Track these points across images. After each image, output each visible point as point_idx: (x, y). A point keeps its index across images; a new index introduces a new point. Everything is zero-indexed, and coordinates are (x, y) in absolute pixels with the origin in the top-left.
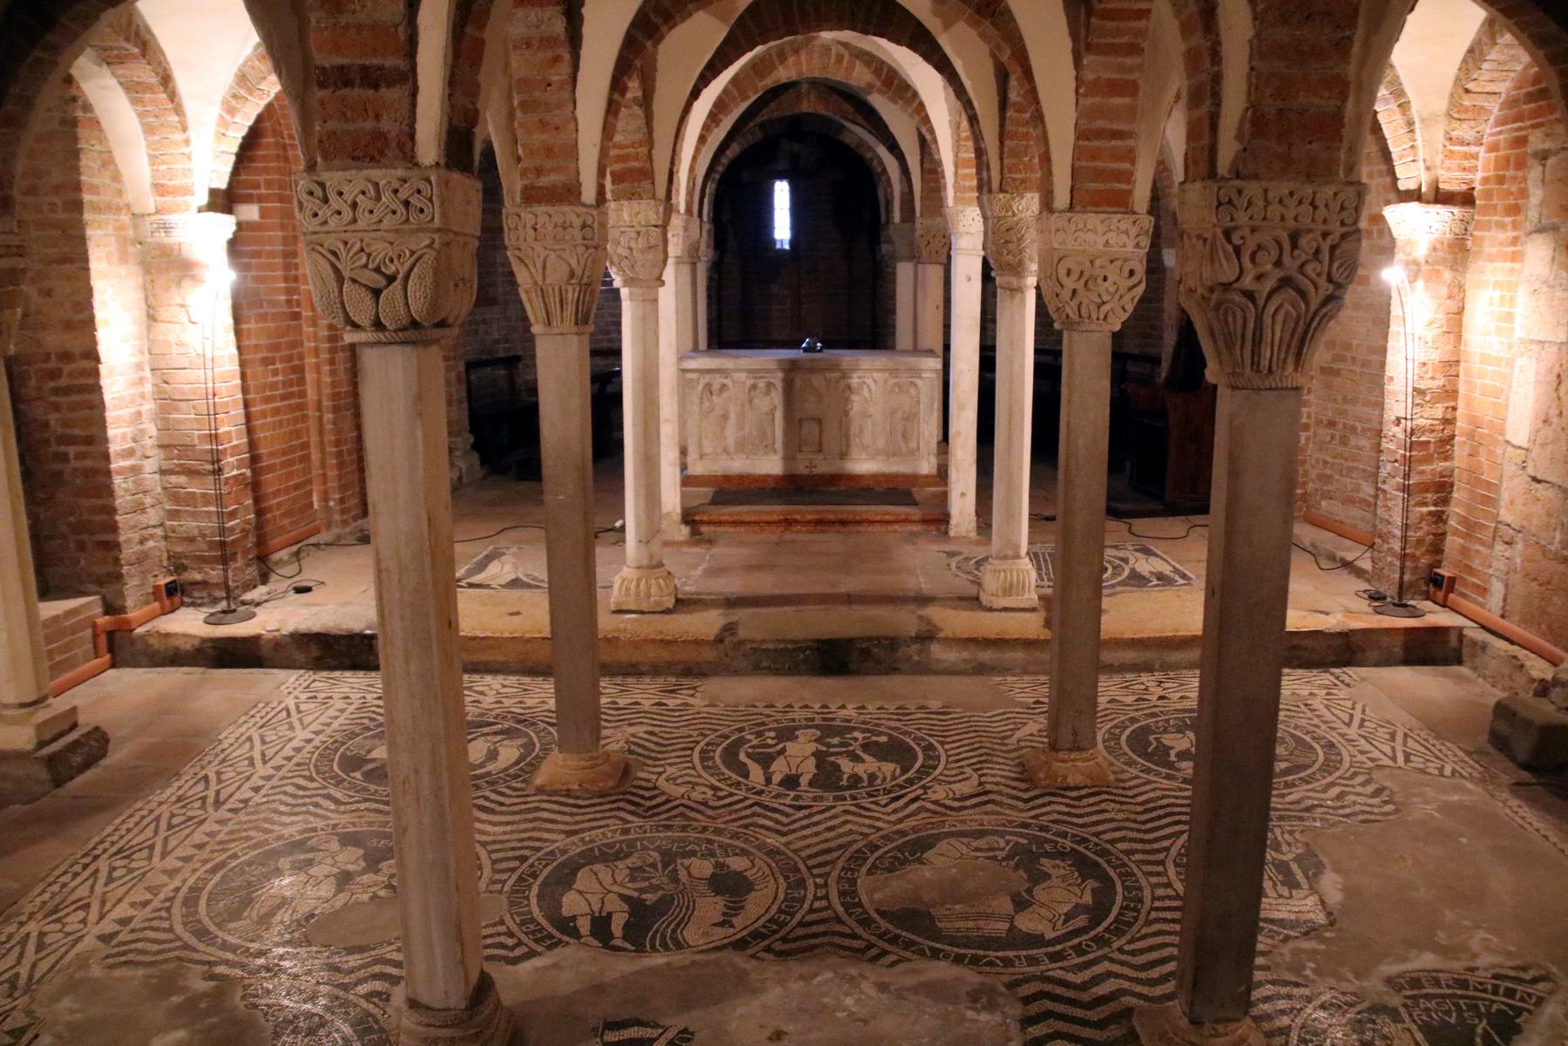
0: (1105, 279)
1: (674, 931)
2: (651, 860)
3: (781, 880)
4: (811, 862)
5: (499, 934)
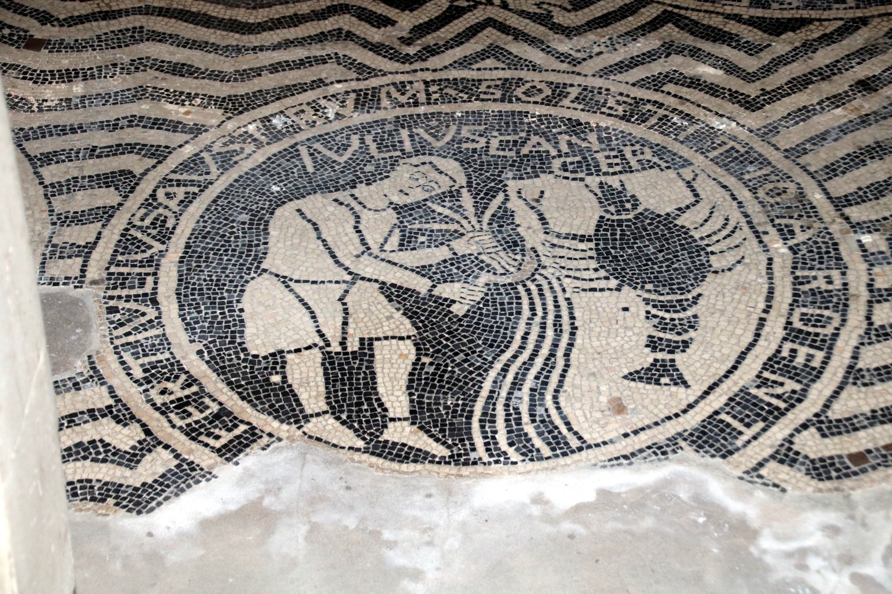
1: (536, 395)
2: (445, 184)
3: (779, 248)
4: (841, 186)
5: (92, 414)
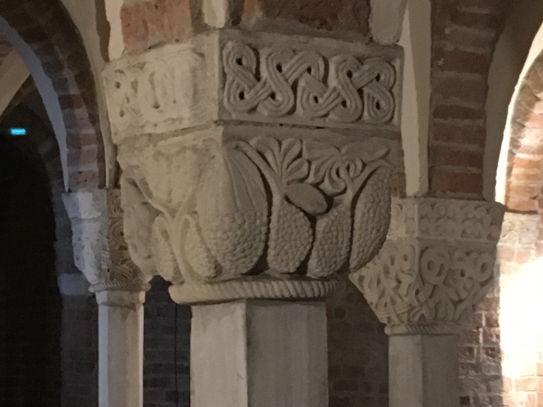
0: (462, 274)
